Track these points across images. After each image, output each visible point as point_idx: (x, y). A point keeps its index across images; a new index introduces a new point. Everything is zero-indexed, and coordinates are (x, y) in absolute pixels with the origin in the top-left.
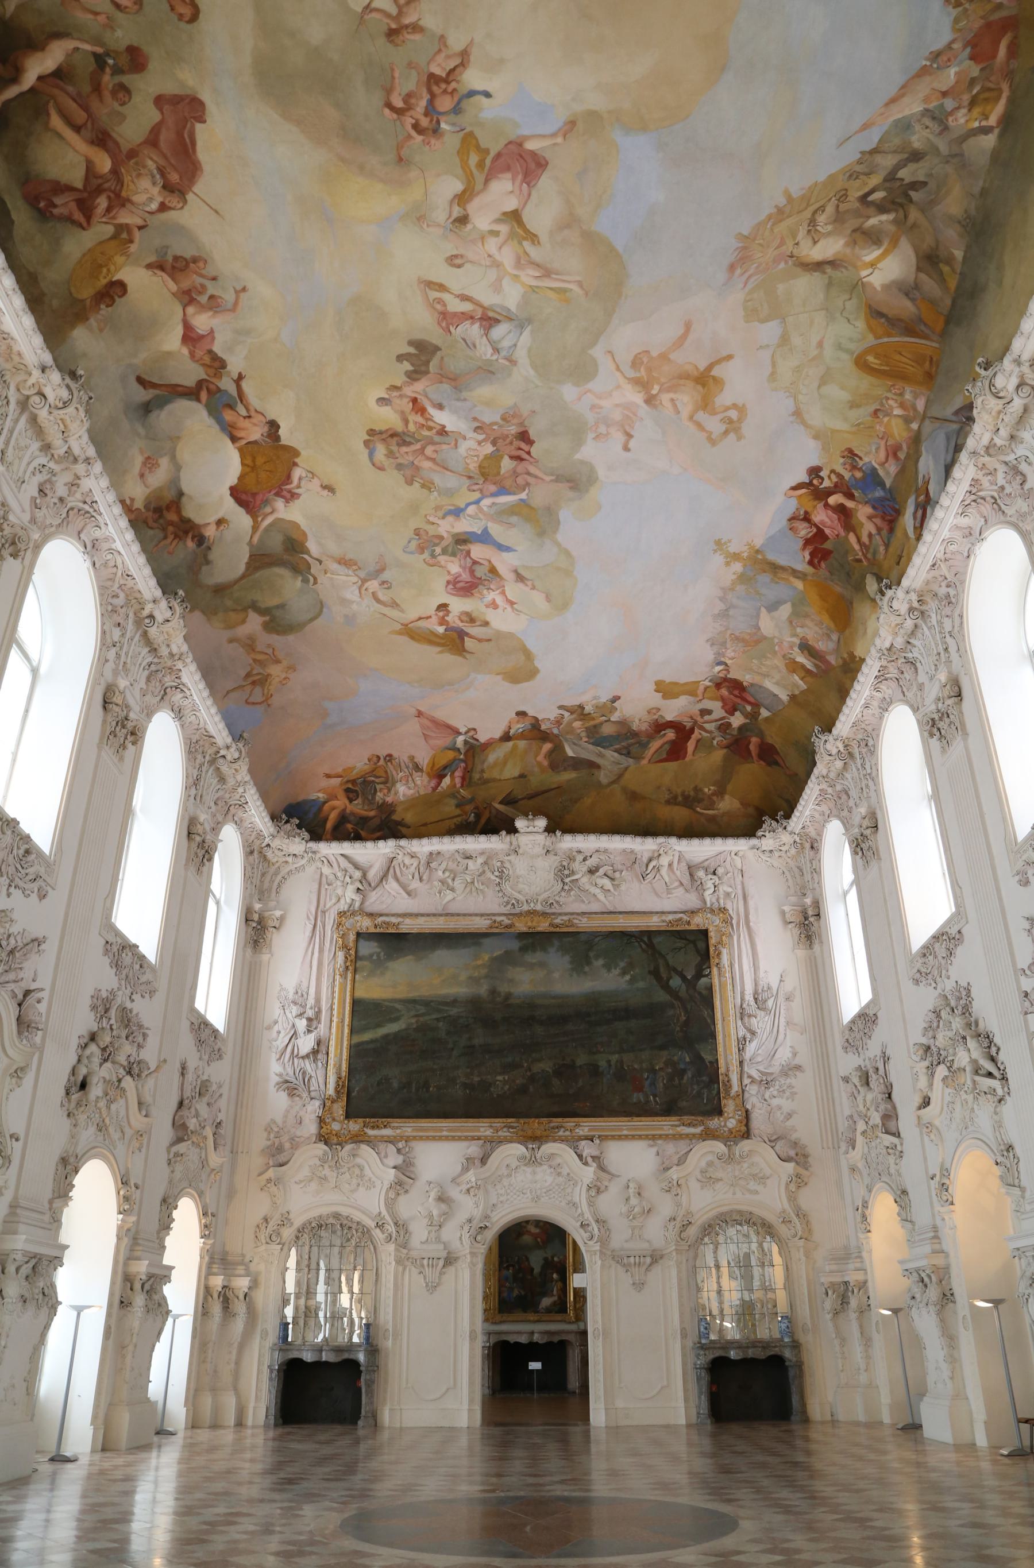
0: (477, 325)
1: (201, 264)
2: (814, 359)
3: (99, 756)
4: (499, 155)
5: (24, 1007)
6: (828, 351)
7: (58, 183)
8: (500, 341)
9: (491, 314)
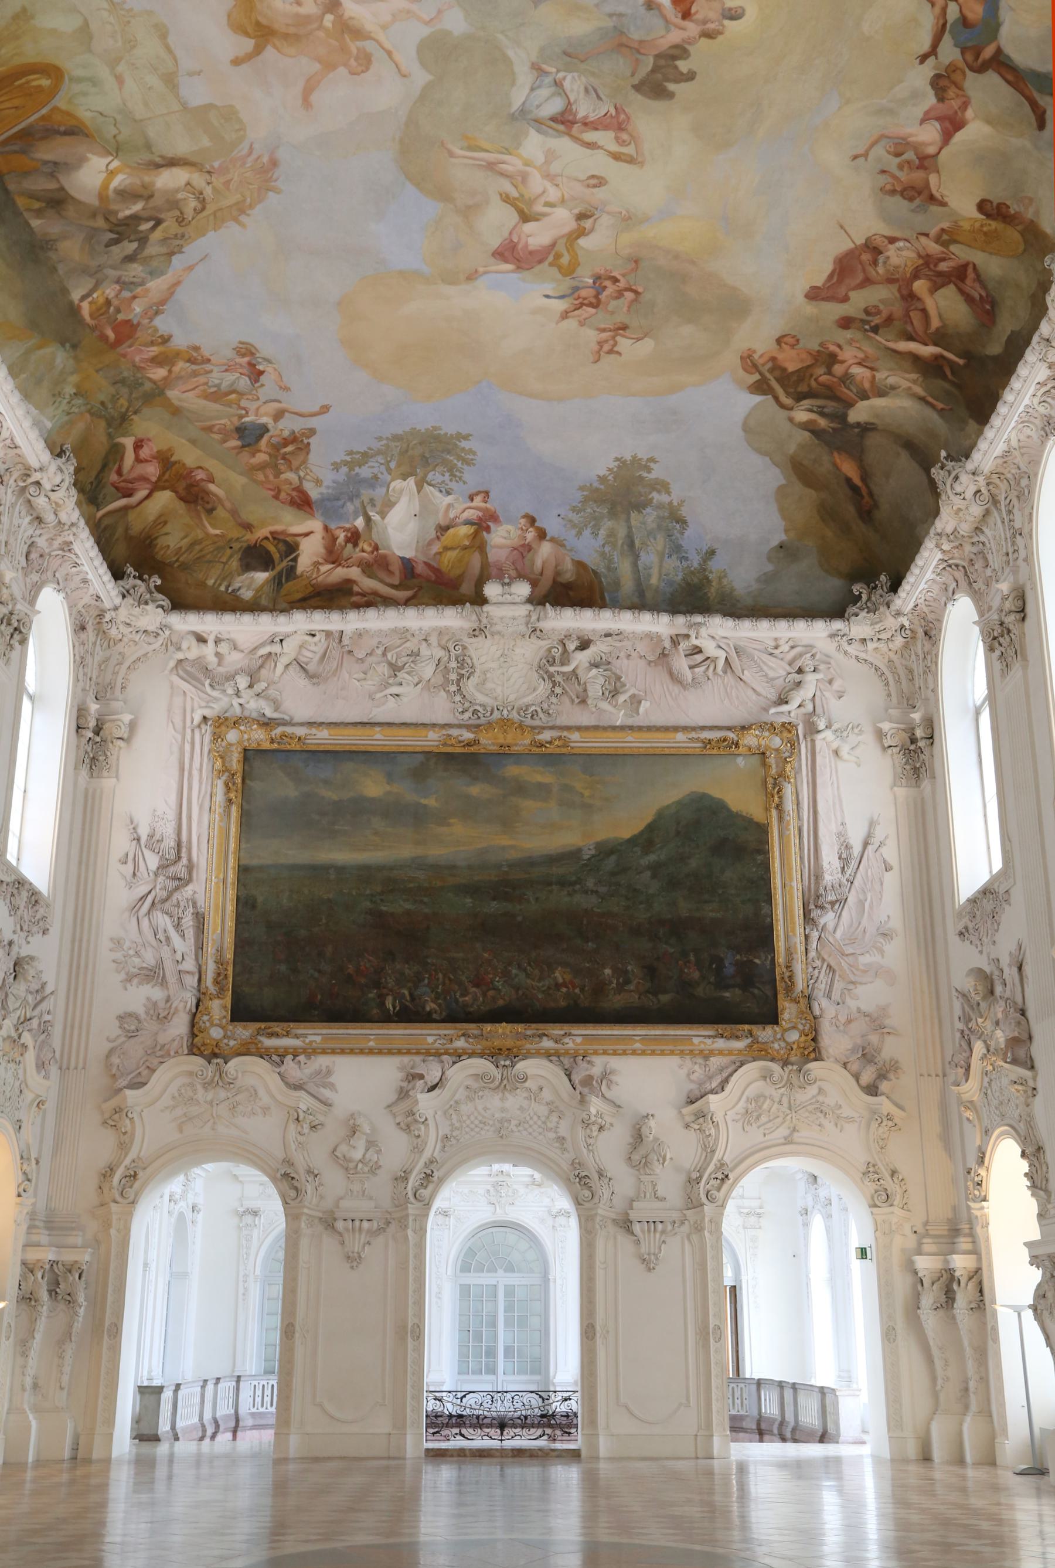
0: (581, 115)
1: (889, 187)
2: (118, 60)
4: (540, 262)
6: (103, 72)
7: (966, 300)
8: (553, 95)
9: (561, 127)
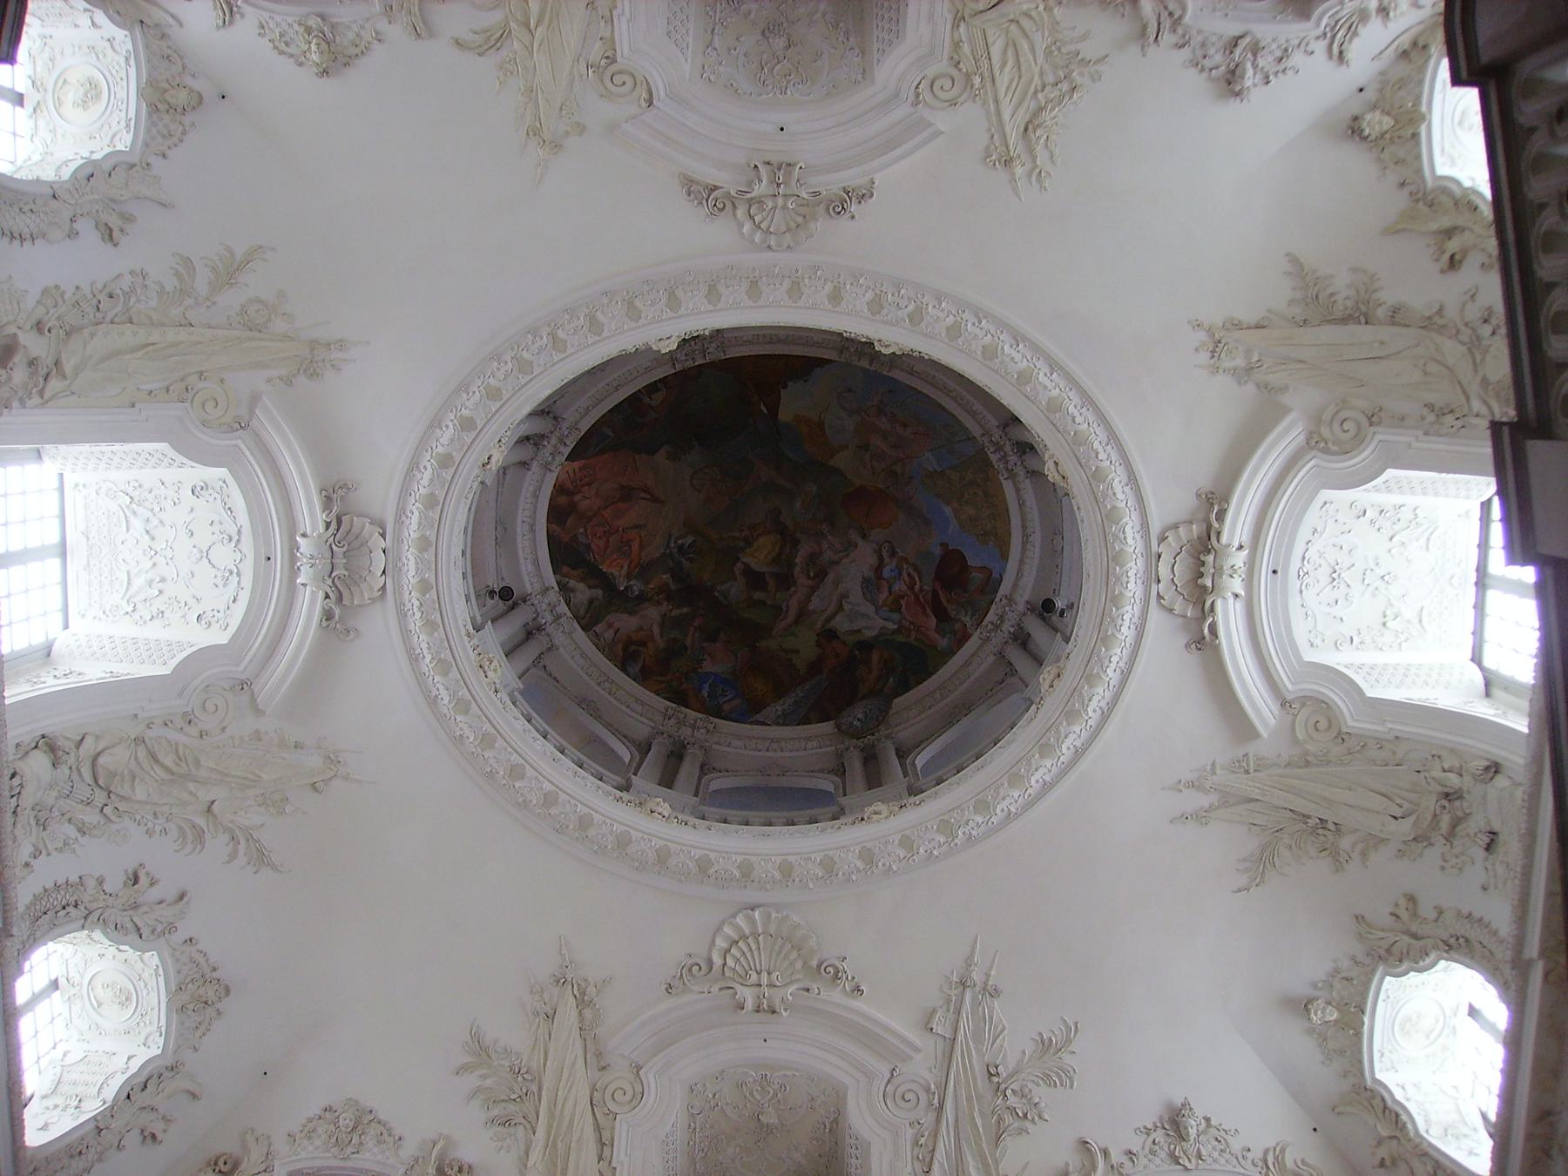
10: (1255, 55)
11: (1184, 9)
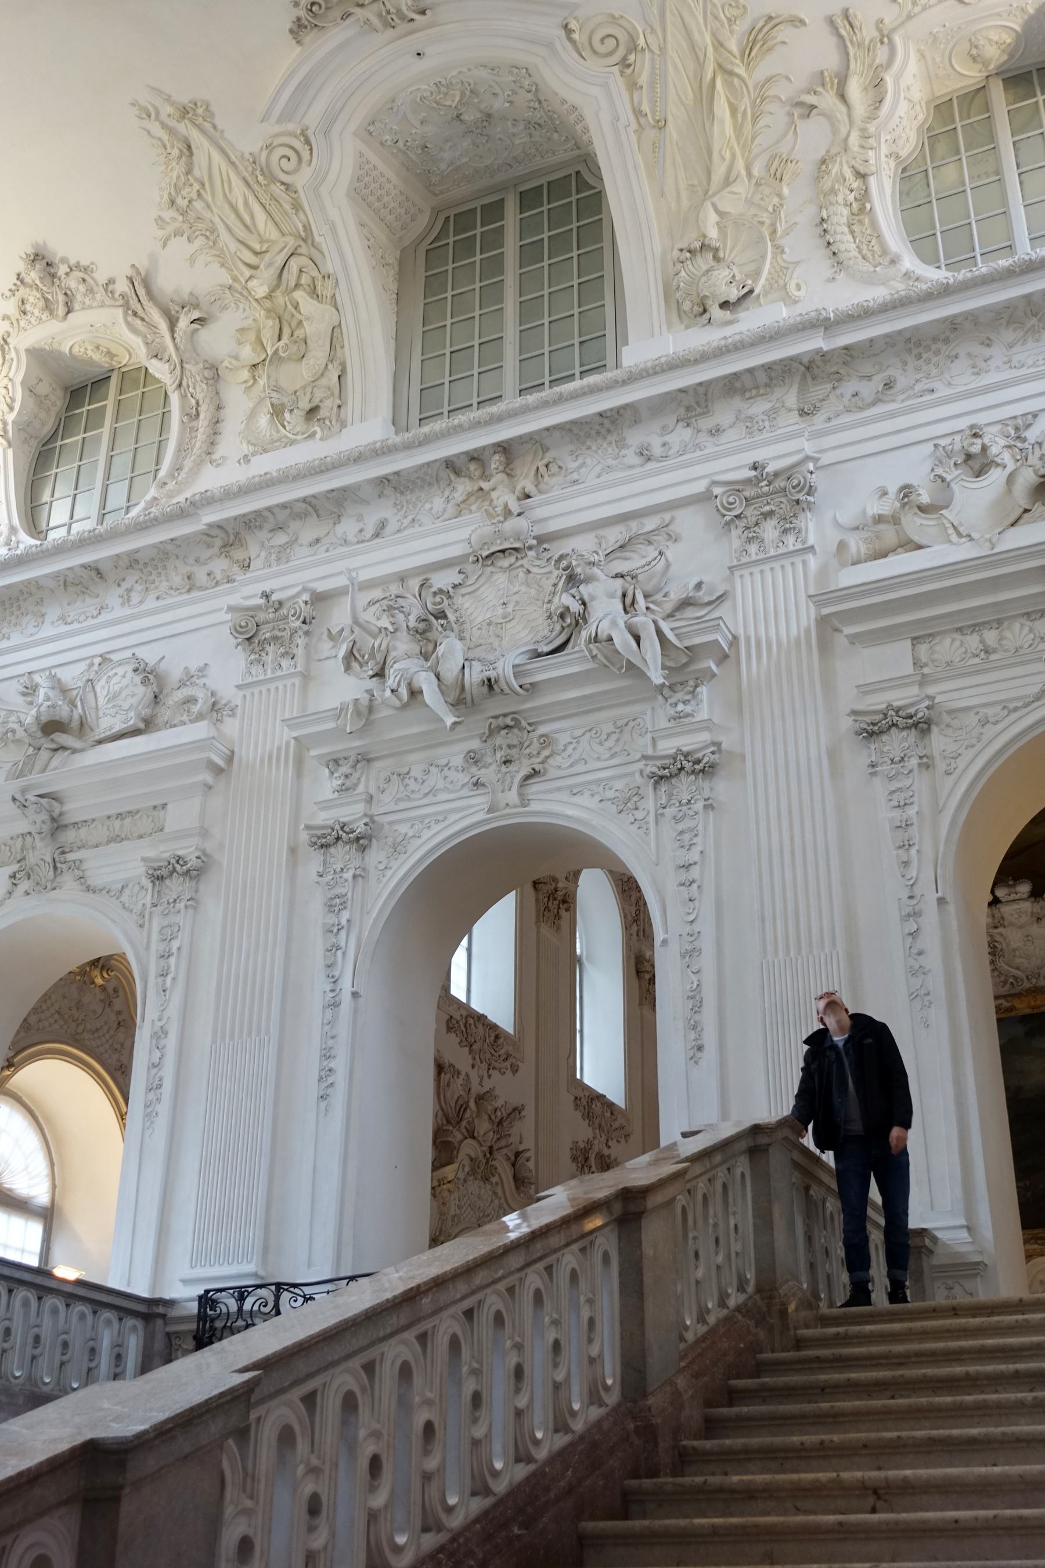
3: (538, 932)
5: (517, 1165)
10: (46, 300)
11: (127, 323)
